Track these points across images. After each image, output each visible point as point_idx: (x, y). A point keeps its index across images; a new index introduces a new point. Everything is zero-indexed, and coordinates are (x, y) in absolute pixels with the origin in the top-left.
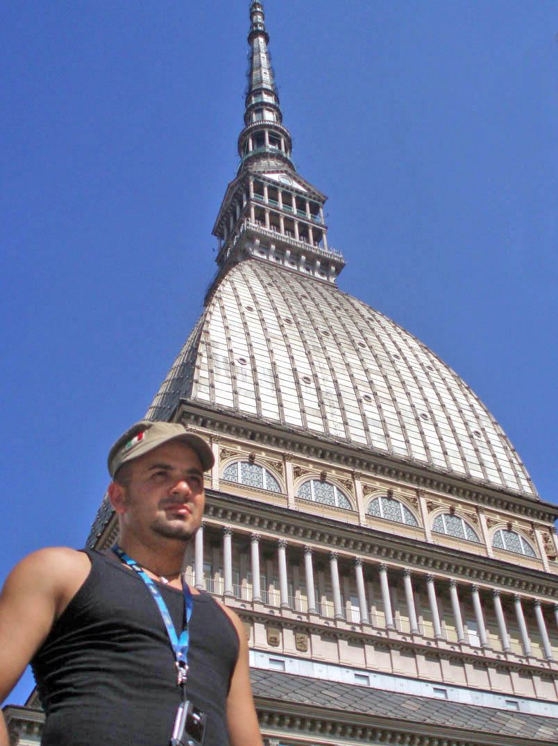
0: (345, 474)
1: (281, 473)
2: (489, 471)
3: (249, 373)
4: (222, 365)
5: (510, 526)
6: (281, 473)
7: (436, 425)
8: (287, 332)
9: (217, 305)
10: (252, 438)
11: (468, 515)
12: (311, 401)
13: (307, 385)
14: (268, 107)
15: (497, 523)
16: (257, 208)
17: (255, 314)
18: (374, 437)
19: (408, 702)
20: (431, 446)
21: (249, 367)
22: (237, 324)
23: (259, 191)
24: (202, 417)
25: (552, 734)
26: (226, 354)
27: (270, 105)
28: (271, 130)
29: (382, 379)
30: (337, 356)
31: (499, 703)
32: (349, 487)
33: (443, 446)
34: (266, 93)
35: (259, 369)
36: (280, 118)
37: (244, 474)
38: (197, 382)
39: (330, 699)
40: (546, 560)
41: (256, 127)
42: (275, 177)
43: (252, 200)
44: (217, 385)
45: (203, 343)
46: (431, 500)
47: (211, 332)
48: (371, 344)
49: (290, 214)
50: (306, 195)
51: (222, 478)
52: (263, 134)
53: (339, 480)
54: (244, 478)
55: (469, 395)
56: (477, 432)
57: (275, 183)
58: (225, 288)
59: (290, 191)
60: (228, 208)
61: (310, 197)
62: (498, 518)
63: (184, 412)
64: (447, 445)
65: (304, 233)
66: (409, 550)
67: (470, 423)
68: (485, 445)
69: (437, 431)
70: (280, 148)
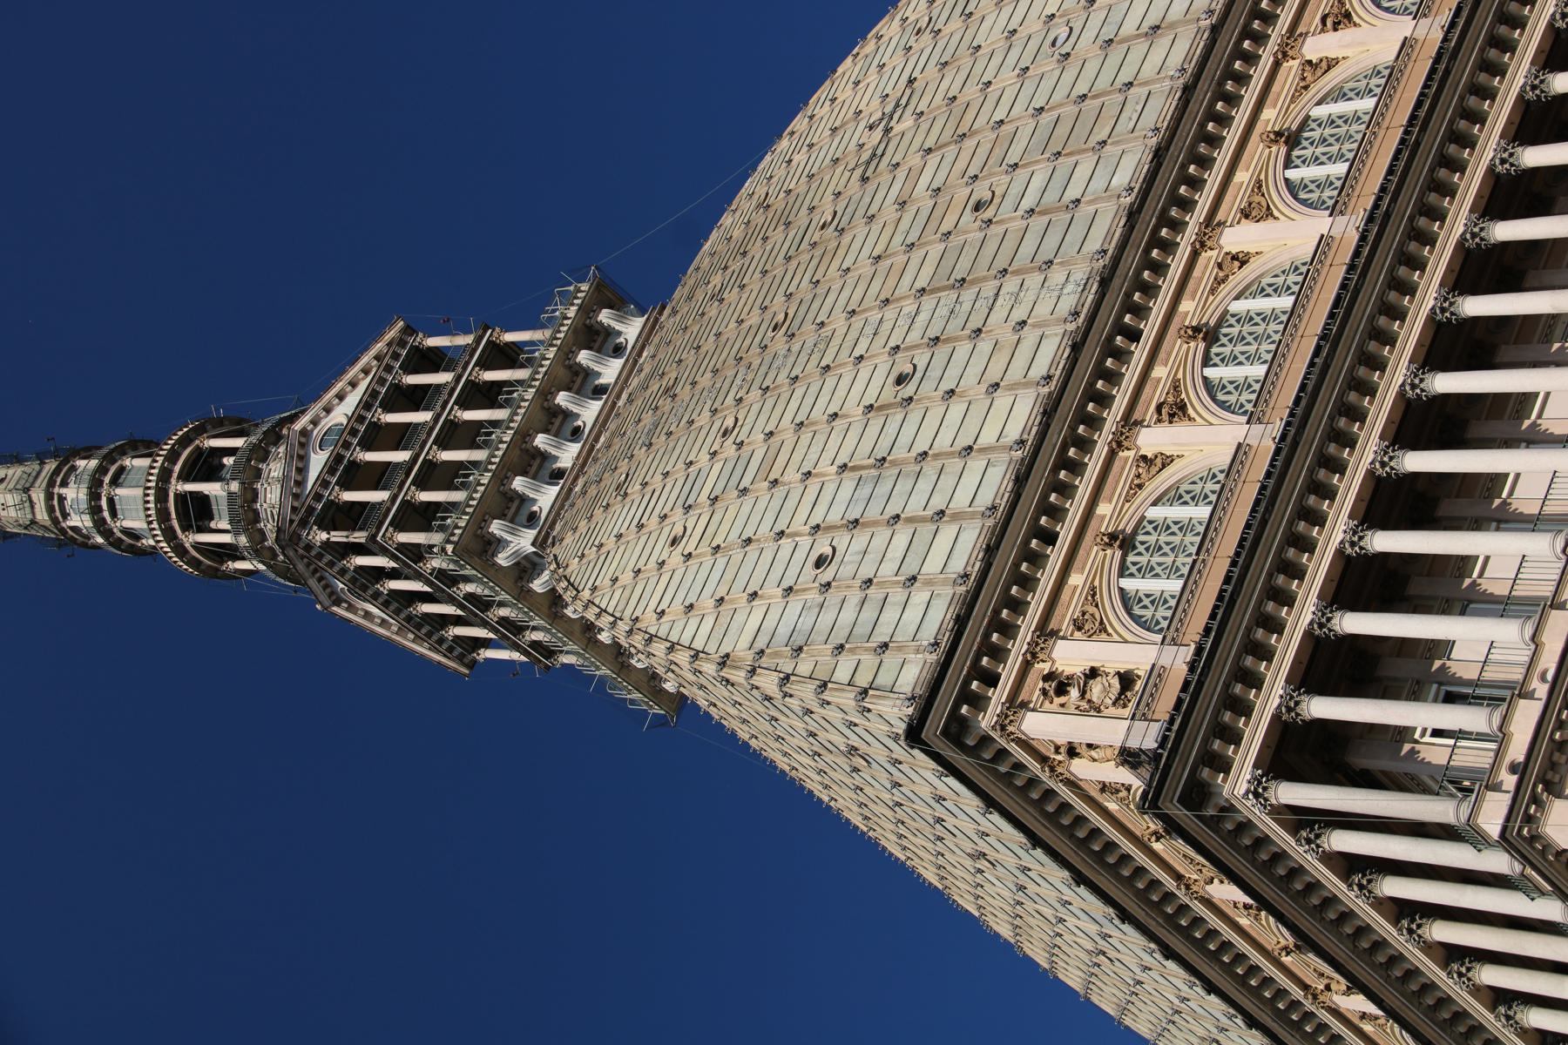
0: (1196, 273)
1: (1167, 461)
3: (861, 539)
4: (827, 618)
6: (1167, 461)
9: (652, 630)
10: (1050, 538)
13: (918, 375)
14: (107, 479)
16: (400, 525)
17: (696, 523)
18: (1098, 184)
21: (842, 540)
23: (354, 515)
24: (967, 682)
26: (795, 604)
27: (102, 470)
28: (175, 475)
29: (933, 160)
32: (1241, 259)
34: (64, 484)
35: (854, 514)
36: (145, 446)
38: (865, 692)
41: (163, 516)
42: (318, 461)
43: (373, 538)
44: (881, 636)
45: (753, 671)
47: (725, 649)
49: (432, 429)
50: (382, 381)
51: (1159, 638)
52: (181, 498)
53: (1213, 291)
54: (1173, 571)
57: (331, 468)
60: (397, 612)
61: (389, 369)
63: (945, 732)
65: (489, 395)
66: (1465, 72)
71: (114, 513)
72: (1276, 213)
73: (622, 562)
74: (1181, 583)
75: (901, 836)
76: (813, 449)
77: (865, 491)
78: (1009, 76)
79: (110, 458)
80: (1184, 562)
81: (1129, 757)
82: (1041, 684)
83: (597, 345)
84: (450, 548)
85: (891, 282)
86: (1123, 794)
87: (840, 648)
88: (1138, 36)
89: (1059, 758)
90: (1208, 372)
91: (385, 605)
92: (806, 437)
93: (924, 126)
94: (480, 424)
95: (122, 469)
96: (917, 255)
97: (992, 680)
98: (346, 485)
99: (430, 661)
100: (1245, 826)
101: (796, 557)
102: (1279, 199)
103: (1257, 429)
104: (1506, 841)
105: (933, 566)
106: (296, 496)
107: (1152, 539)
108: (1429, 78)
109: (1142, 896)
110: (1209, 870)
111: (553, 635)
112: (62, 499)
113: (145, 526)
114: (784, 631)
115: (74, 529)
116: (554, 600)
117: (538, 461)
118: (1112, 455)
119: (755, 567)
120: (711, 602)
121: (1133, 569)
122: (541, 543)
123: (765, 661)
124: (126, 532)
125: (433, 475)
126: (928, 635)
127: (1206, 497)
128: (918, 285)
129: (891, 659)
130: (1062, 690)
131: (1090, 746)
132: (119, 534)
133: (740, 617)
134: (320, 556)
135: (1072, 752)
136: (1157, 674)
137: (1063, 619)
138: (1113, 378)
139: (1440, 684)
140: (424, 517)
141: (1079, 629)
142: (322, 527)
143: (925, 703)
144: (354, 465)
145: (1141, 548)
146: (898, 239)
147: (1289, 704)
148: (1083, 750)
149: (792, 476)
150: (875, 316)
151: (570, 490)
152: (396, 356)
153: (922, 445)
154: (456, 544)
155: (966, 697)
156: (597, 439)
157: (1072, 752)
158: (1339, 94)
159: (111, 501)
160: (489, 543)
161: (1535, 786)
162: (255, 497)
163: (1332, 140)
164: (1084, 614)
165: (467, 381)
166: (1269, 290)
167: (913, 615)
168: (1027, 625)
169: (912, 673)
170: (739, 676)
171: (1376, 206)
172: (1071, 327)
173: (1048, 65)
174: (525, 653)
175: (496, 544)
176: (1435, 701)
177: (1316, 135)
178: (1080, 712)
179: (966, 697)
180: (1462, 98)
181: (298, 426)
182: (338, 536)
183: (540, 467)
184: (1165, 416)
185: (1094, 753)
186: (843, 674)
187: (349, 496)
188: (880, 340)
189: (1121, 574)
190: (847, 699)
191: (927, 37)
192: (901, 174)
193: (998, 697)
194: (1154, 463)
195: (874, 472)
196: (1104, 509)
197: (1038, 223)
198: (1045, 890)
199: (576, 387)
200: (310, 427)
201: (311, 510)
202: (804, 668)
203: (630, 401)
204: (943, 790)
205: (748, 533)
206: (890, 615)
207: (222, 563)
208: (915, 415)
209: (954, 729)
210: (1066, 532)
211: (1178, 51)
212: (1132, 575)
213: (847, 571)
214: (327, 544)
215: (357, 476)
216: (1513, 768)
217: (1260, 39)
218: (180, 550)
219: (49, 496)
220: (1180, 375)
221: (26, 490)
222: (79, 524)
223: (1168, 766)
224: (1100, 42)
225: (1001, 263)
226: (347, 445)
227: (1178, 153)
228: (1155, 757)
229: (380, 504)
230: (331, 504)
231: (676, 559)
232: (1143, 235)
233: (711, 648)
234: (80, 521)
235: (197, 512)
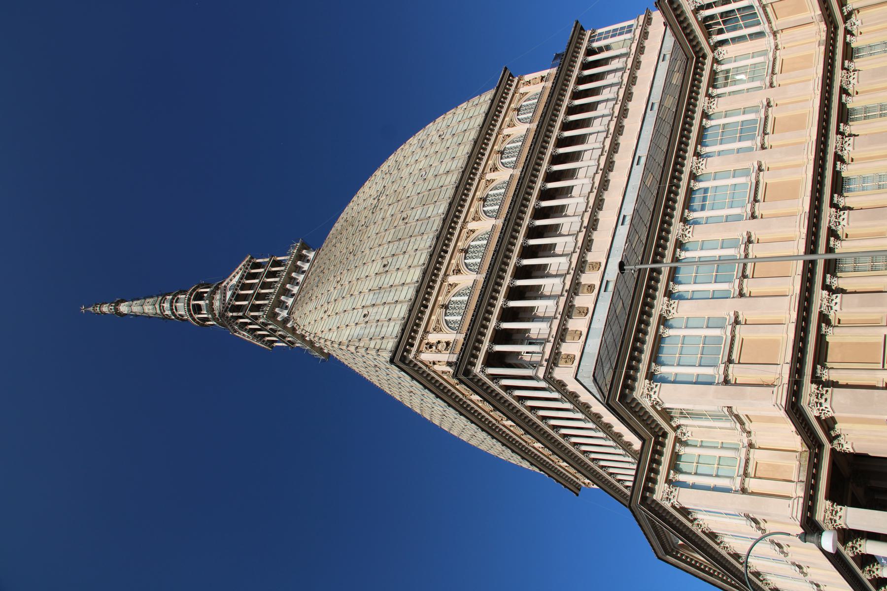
1: (456, 285)
2: (470, 127)
3: (375, 309)
4: (367, 331)
6: (456, 285)
10: (426, 307)
12: (402, 261)
13: (389, 264)
14: (174, 301)
16: (251, 310)
17: (331, 306)
18: (435, 212)
19: (646, 183)
21: (370, 310)
22: (337, 321)
23: (239, 308)
24: (405, 346)
25: (678, 74)
26: (359, 327)
27: (173, 299)
28: (192, 299)
29: (391, 207)
31: (652, 117)
32: (473, 231)
34: (164, 303)
36: (183, 292)
38: (378, 350)
39: (639, 240)
40: (543, 84)
41: (189, 310)
42: (229, 294)
43: (244, 314)
45: (348, 346)
46: (489, 169)
49: (259, 284)
50: (245, 272)
51: (456, 332)
52: (194, 305)
53: (466, 240)
54: (459, 314)
56: (440, 136)
57: (232, 296)
59: (240, 285)
60: (252, 334)
61: (247, 268)
63: (400, 360)
70: (206, 292)
71: (177, 310)
72: (481, 219)
73: (311, 318)
74: (461, 317)
75: (390, 388)
76: (362, 285)
77: (376, 296)
78: (410, 185)
79: (175, 296)
80: (462, 311)
81: (449, 364)
82: (425, 346)
83: (302, 260)
84: (265, 316)
85: (381, 240)
86: (448, 374)
89: (431, 365)
90: (466, 261)
91: (248, 332)
92: (360, 282)
93: (388, 198)
94: (271, 282)
95: (178, 298)
96: (388, 232)
97: (412, 345)
98: (237, 300)
99: (261, 347)
100: (480, 380)
101: (358, 315)
102: (482, 215)
103: (479, 275)
104: (545, 379)
105: (395, 316)
106: (223, 304)
107: (453, 306)
108: (518, 184)
109: (454, 400)
110: (471, 392)
111: (294, 339)
112: (163, 307)
113: (185, 313)
114: (356, 335)
115: (166, 315)
116: (293, 329)
117: (288, 292)
118: (442, 284)
119: (347, 318)
120: (336, 328)
121: (448, 314)
122: (289, 314)
123: (351, 343)
124: (180, 315)
125: (260, 297)
126: (394, 334)
127: (467, 294)
128: (388, 240)
130: (431, 347)
131: (439, 361)
132: (178, 316)
133: (344, 332)
134: (230, 320)
135: (434, 363)
136: (456, 341)
137: (430, 328)
138: (441, 263)
139: (528, 340)
140: (257, 308)
141: (435, 331)
142: (230, 312)
143: (395, 353)
144: (238, 295)
145: (450, 308)
146: (382, 228)
147: (490, 348)
149: (356, 293)
150: (377, 249)
151: (297, 299)
152: (249, 265)
153: (391, 283)
154: (266, 315)
155: (405, 350)
156: (303, 285)
157: (434, 363)
158: (495, 188)
159: (176, 307)
160: (275, 314)
161: (551, 365)
162: (213, 305)
163: (494, 200)
164: (436, 326)
165: (268, 271)
166: (481, 239)
167: (390, 329)
168: (421, 330)
169: (390, 344)
170: (344, 347)
171: (506, 217)
172: (429, 250)
173: (421, 182)
174: (286, 344)
175: (277, 314)
176: (527, 344)
177: (490, 199)
178: (437, 353)
179: (405, 350)
180: (526, 189)
181: (223, 285)
182: (235, 314)
183: (288, 293)
184: (455, 273)
185: (440, 363)
186: (372, 346)
187: (237, 303)
188: (379, 256)
189: (445, 316)
190: (374, 352)
191: (388, 175)
192: (383, 211)
193: (414, 350)
195: (378, 291)
196: (440, 298)
197: (419, 223)
198: (428, 400)
199: (297, 271)
200: (226, 285)
201: (227, 307)
202: (362, 344)
203: (312, 274)
204: (401, 376)
206: (384, 329)
207: (205, 322)
208: (389, 276)
209: (402, 359)
210: (430, 305)
211: (454, 178)
212: (448, 316)
213: (372, 318)
214: (232, 316)
215: (239, 297)
216: (546, 360)
217: (475, 174)
218: (194, 319)
219: (160, 306)
220: (459, 262)
221: (154, 305)
222: (168, 313)
223: (459, 366)
224: (434, 175)
225: (410, 234)
226: (236, 289)
227: (455, 204)
228: (456, 363)
229: (246, 305)
230: (233, 305)
231: (326, 316)
232: (447, 226)
233: (336, 340)
234: (168, 312)
235: (198, 309)
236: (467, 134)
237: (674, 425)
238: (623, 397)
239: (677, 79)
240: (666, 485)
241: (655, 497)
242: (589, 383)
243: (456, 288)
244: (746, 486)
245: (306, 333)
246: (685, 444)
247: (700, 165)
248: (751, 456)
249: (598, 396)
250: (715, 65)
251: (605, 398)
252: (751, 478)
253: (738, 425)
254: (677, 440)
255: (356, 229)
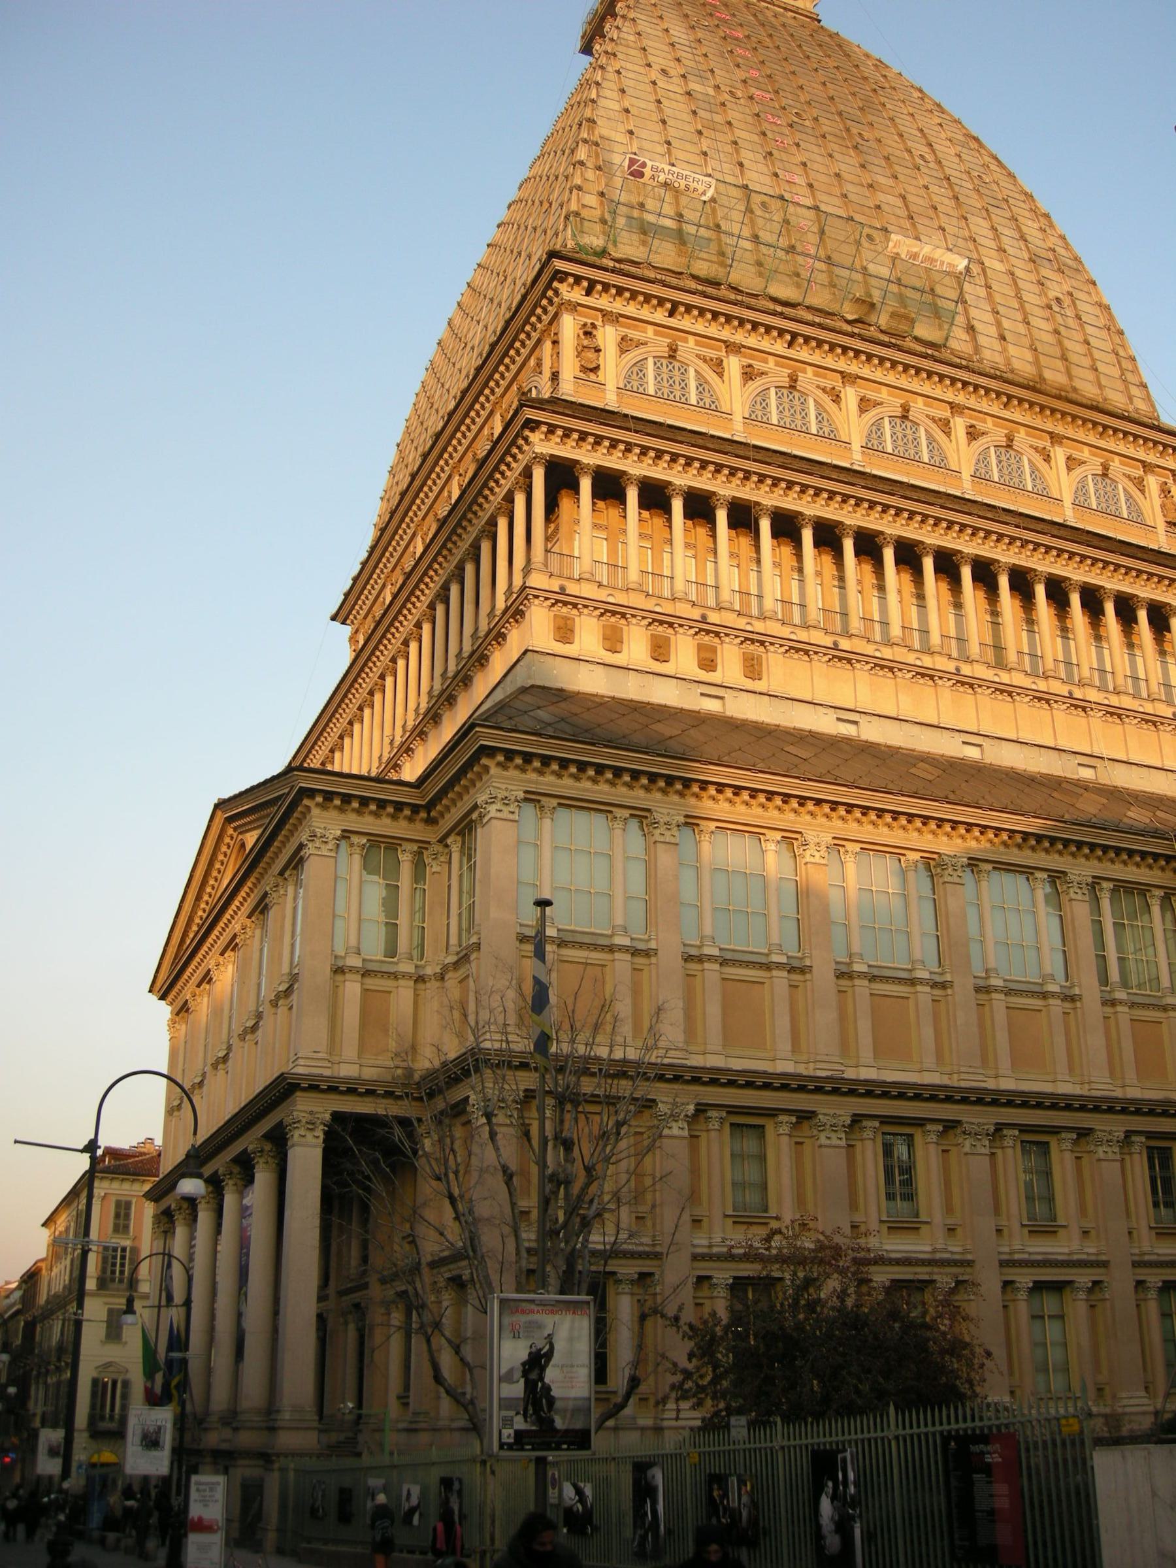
1: (720, 375)
2: (1075, 371)
5: (1106, 468)
6: (720, 375)
7: (988, 287)
8: (732, 115)
9: (609, 69)
11: (1036, 449)
13: (767, 216)
15: (1084, 462)
19: (921, 764)
20: (978, 326)
29: (899, 202)
30: (819, 159)
32: (837, 399)
33: (999, 324)
37: (659, 379)
39: (797, 760)
45: (585, 141)
46: (974, 422)
48: (878, 134)
51: (621, 386)
53: (818, 387)
55: (1047, 229)
56: (1058, 299)
58: (622, 35)
62: (1086, 453)
63: (558, 272)
64: (1006, 324)
67: (1048, 283)
68: (1072, 323)
69: (990, 298)
87: (602, 194)
88: (968, 320)
104: (524, 587)
121: (658, 364)
129: (598, 227)
135: (555, 343)
145: (670, 367)
148: (556, 351)
149: (705, 145)
157: (555, 343)
158: (931, 440)
179: (578, 279)
190: (574, 207)
192: (891, 182)
194: (718, 367)
205: (670, 122)
223: (544, 410)
231: (654, 75)
236: (1059, 364)
237: (449, 841)
238: (490, 751)
239: (1137, 816)
240: (339, 833)
241: (315, 811)
242: (520, 679)
243: (714, 376)
244: (348, 976)
245: (617, 28)
246: (419, 867)
247: (950, 870)
248: (402, 982)
249: (499, 696)
250: (1161, 893)
251: (485, 720)
252: (362, 984)
253: (452, 959)
254: (423, 845)
255: (854, 118)
